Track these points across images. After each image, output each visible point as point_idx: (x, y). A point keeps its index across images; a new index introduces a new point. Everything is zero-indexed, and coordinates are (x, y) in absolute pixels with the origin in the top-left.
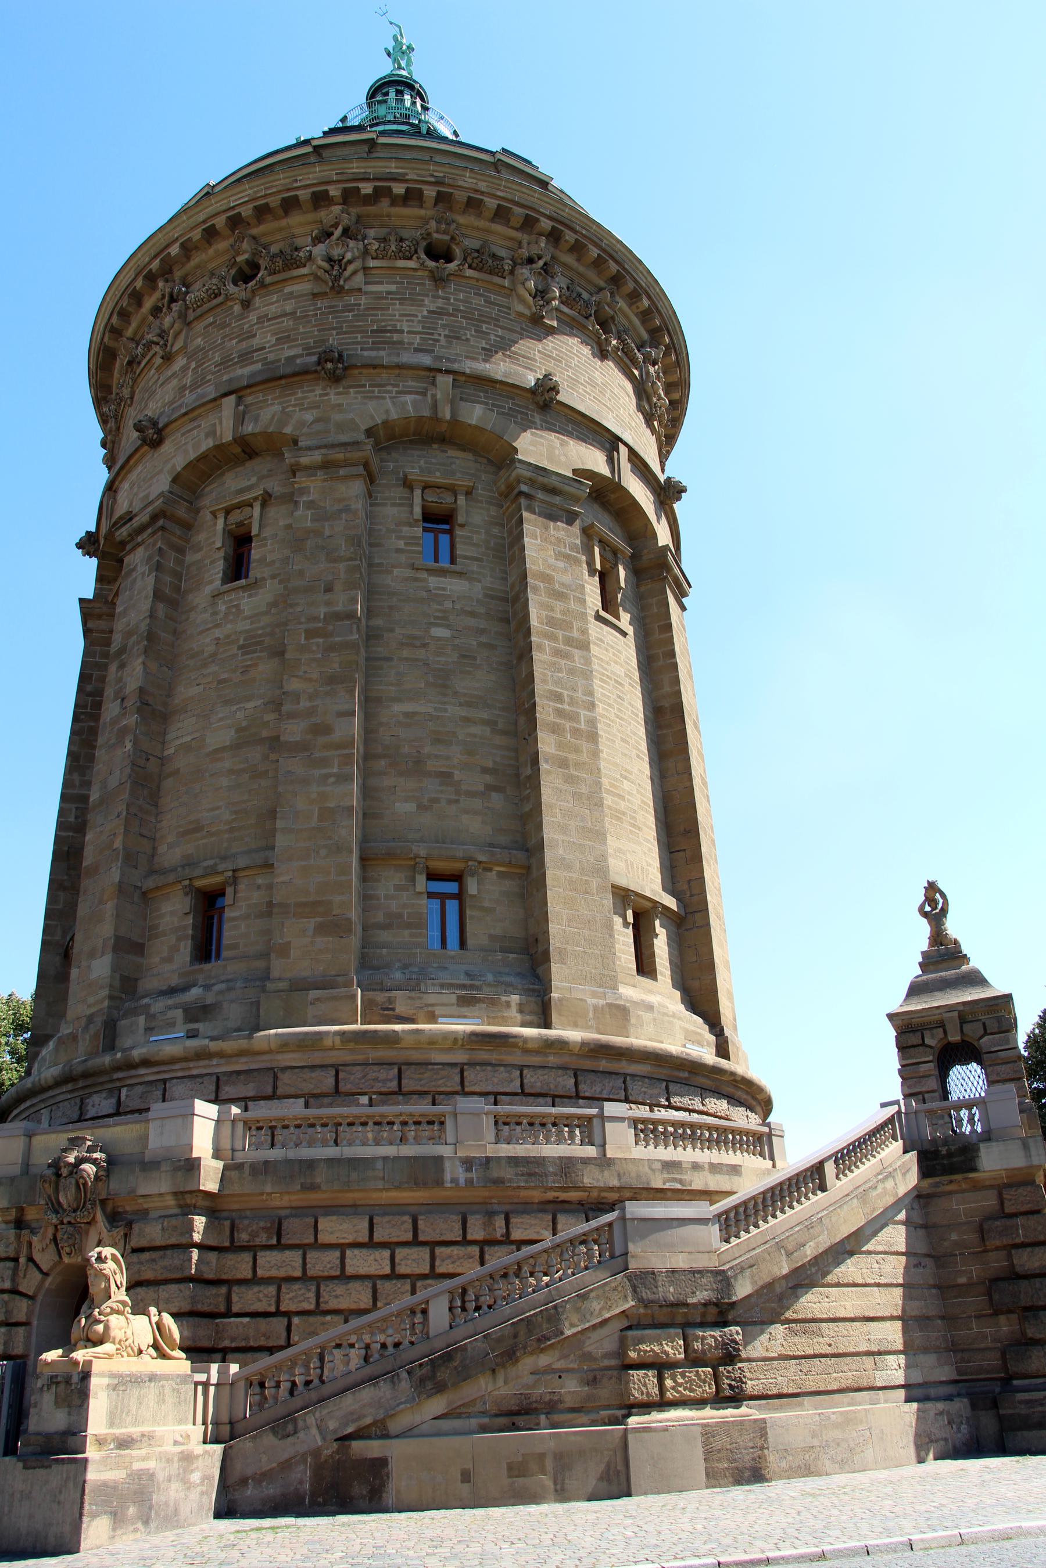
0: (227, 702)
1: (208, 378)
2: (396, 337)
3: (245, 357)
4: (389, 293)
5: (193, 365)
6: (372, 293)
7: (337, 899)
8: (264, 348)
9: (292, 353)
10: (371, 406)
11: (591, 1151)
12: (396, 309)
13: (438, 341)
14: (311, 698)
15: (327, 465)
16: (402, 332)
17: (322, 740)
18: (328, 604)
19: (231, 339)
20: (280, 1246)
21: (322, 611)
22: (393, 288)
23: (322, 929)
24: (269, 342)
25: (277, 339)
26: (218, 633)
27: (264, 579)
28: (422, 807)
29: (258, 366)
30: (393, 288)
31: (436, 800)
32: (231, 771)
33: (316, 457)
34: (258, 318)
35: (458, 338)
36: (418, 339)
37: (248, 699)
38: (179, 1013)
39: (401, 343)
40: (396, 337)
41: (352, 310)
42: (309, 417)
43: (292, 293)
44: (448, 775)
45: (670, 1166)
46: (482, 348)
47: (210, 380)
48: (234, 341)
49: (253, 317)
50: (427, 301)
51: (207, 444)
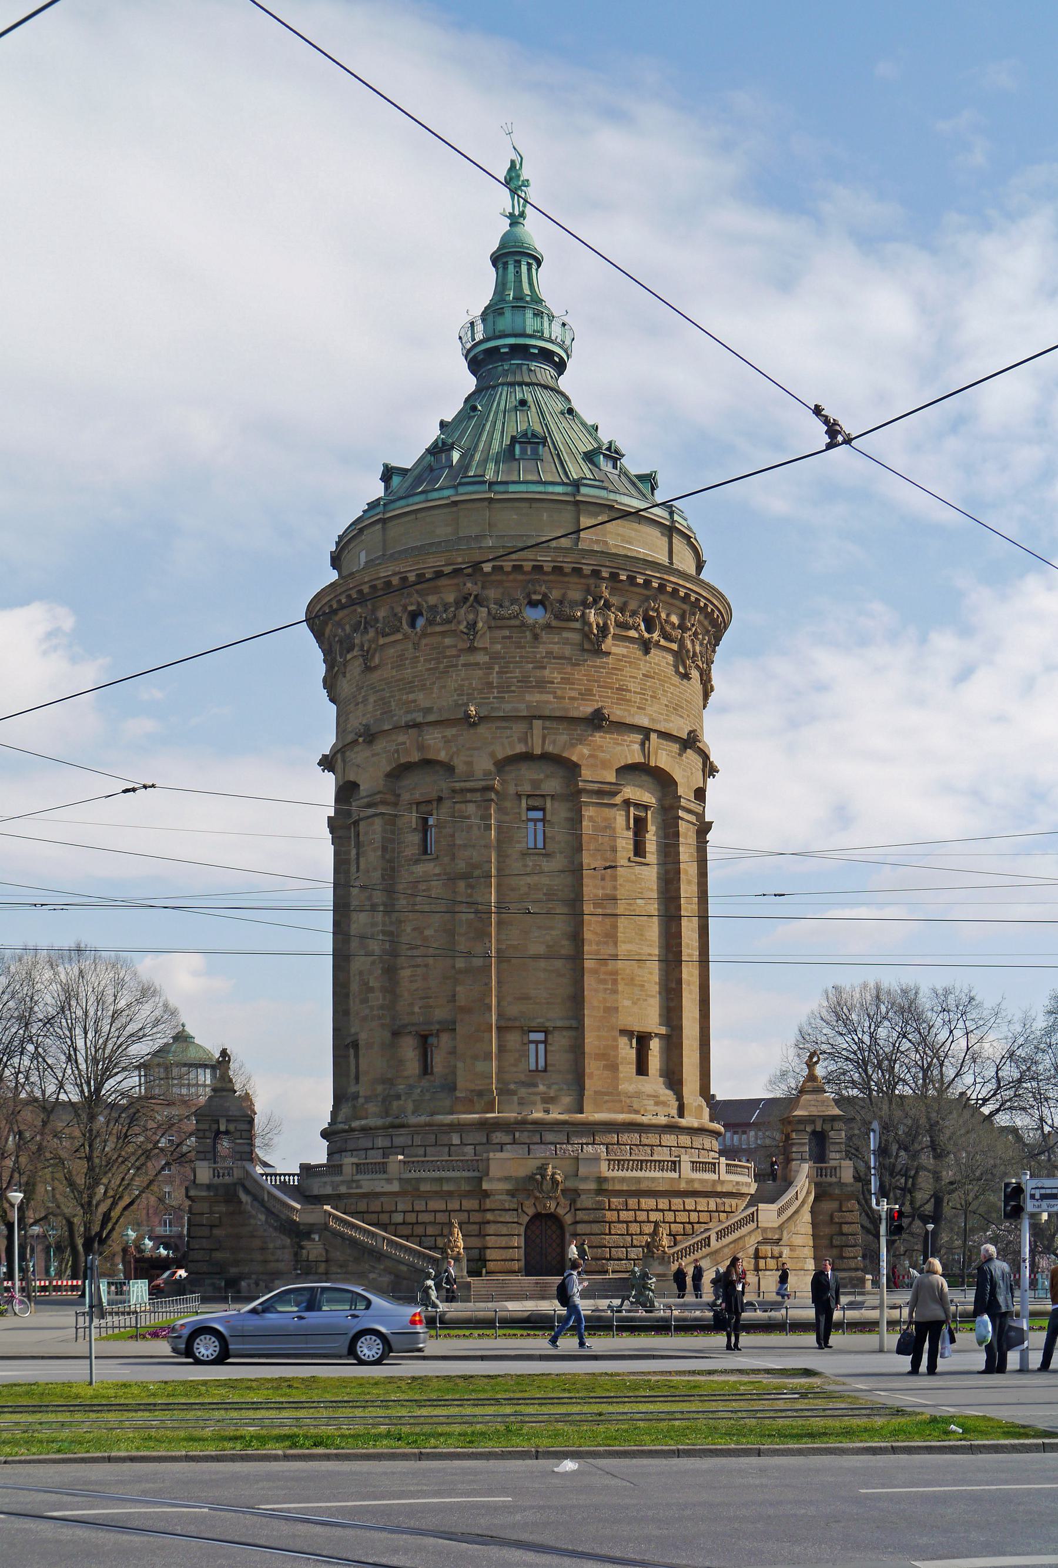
0: (539, 927)
1: (513, 688)
2: (628, 696)
3: (542, 685)
4: (624, 656)
5: (497, 668)
6: (615, 654)
7: (612, 1053)
8: (553, 683)
9: (574, 694)
10: (619, 748)
11: (716, 1177)
12: (628, 671)
13: (647, 700)
14: (598, 943)
15: (600, 793)
16: (629, 691)
17: (603, 969)
18: (603, 888)
19: (528, 662)
20: (627, 1210)
21: (600, 892)
22: (624, 651)
23: (606, 1067)
24: (556, 678)
25: (562, 678)
26: (529, 880)
27: (554, 852)
28: (634, 1003)
29: (550, 698)
30: (624, 651)
31: (638, 999)
32: (545, 970)
33: (595, 787)
34: (547, 653)
35: (655, 697)
36: (637, 698)
37: (552, 928)
38: (538, 1098)
39: (629, 701)
40: (628, 696)
41: (604, 668)
42: (586, 752)
43: (567, 639)
44: (643, 986)
45: (738, 1183)
46: (666, 706)
47: (514, 692)
48: (531, 666)
49: (542, 650)
50: (642, 663)
51: (520, 748)
